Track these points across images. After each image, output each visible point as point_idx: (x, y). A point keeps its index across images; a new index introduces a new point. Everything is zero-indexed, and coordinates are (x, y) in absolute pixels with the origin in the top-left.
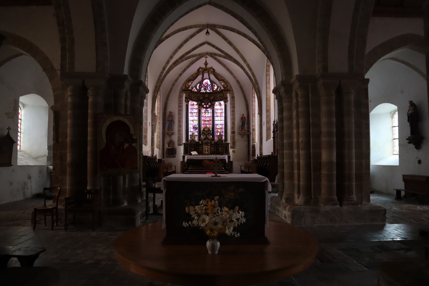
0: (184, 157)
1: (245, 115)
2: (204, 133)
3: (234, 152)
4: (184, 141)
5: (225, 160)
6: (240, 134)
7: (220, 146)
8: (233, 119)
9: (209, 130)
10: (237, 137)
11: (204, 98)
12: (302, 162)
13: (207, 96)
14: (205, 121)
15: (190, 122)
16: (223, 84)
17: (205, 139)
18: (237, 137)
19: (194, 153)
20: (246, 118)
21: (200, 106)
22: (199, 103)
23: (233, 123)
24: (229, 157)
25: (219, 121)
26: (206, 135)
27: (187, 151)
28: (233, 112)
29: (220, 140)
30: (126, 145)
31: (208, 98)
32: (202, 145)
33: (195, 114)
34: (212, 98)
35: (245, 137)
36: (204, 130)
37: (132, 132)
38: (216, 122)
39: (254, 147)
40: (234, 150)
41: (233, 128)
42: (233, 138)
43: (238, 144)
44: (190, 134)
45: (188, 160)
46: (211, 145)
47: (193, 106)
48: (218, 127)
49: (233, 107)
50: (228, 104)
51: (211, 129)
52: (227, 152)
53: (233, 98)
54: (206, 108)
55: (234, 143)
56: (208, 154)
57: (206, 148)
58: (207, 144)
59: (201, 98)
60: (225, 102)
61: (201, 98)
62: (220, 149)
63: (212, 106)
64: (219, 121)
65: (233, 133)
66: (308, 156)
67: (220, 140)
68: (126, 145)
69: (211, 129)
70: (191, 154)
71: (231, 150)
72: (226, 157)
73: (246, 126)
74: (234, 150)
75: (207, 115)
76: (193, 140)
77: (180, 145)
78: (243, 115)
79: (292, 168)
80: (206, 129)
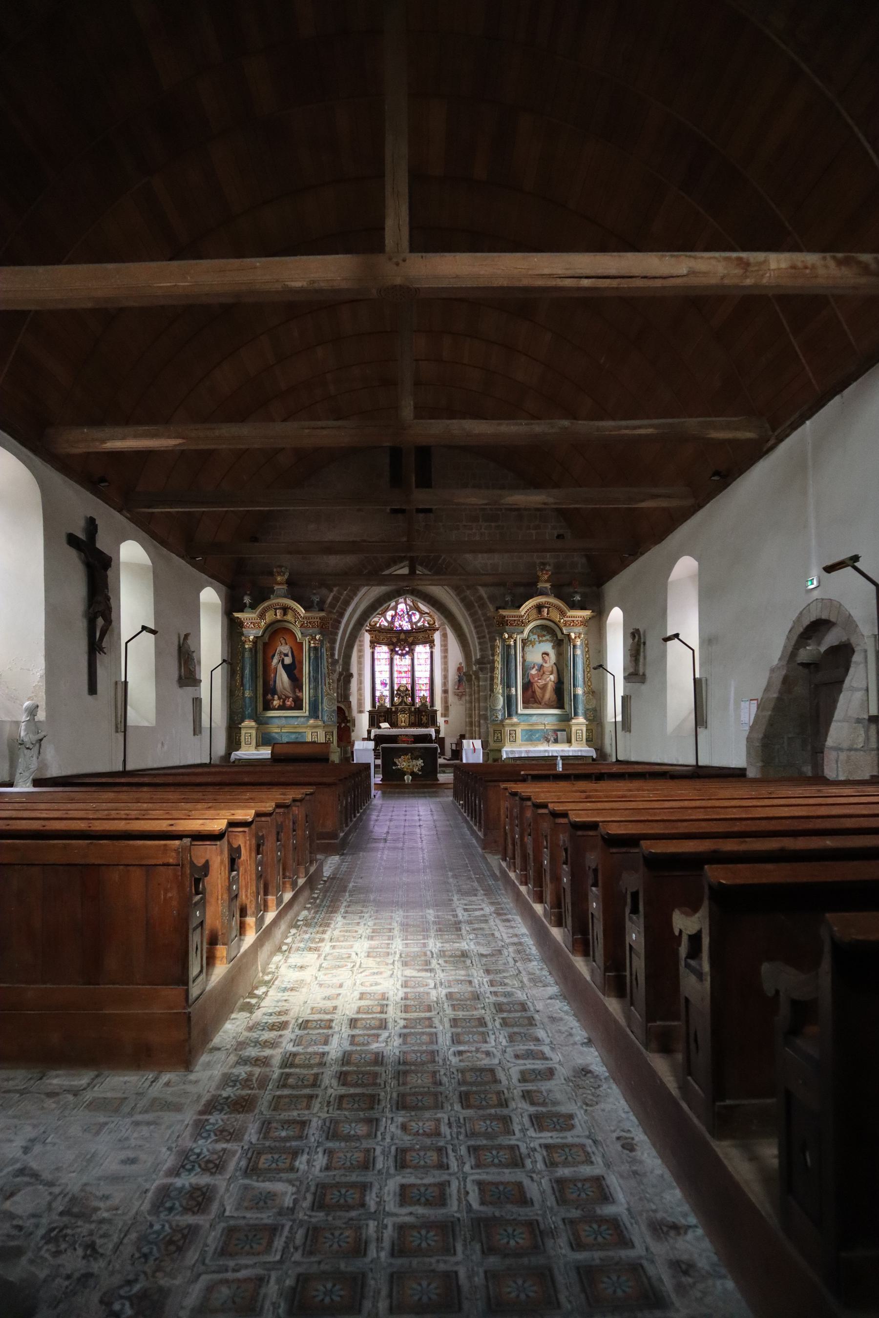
0: (369, 732)
2: (400, 695)
3: (446, 722)
4: (368, 707)
5: (431, 735)
6: (456, 694)
7: (424, 715)
8: (445, 670)
9: (407, 689)
10: (451, 698)
11: (399, 640)
13: (402, 636)
14: (400, 672)
15: (377, 675)
17: (400, 704)
19: (385, 725)
21: (393, 651)
22: (392, 647)
23: (445, 677)
25: (422, 673)
26: (403, 697)
27: (374, 722)
28: (445, 658)
29: (424, 705)
30: (343, 725)
31: (405, 641)
32: (396, 712)
33: (383, 662)
34: (410, 640)
36: (399, 690)
37: (347, 714)
38: (417, 674)
40: (446, 719)
41: (445, 684)
42: (445, 701)
43: (453, 711)
44: (378, 694)
45: (375, 736)
46: (410, 712)
47: (382, 651)
48: (421, 682)
50: (437, 650)
51: (410, 688)
54: (402, 655)
55: (446, 708)
56: (405, 727)
57: (403, 718)
58: (403, 711)
59: (395, 640)
61: (395, 640)
62: (424, 719)
63: (411, 652)
64: (422, 673)
65: (445, 692)
67: (424, 705)
68: (343, 725)
69: (410, 688)
70: (380, 728)
71: (440, 720)
72: (432, 731)
74: (446, 719)
75: (402, 663)
76: (382, 705)
77: (361, 712)
78: (460, 664)
80: (402, 689)
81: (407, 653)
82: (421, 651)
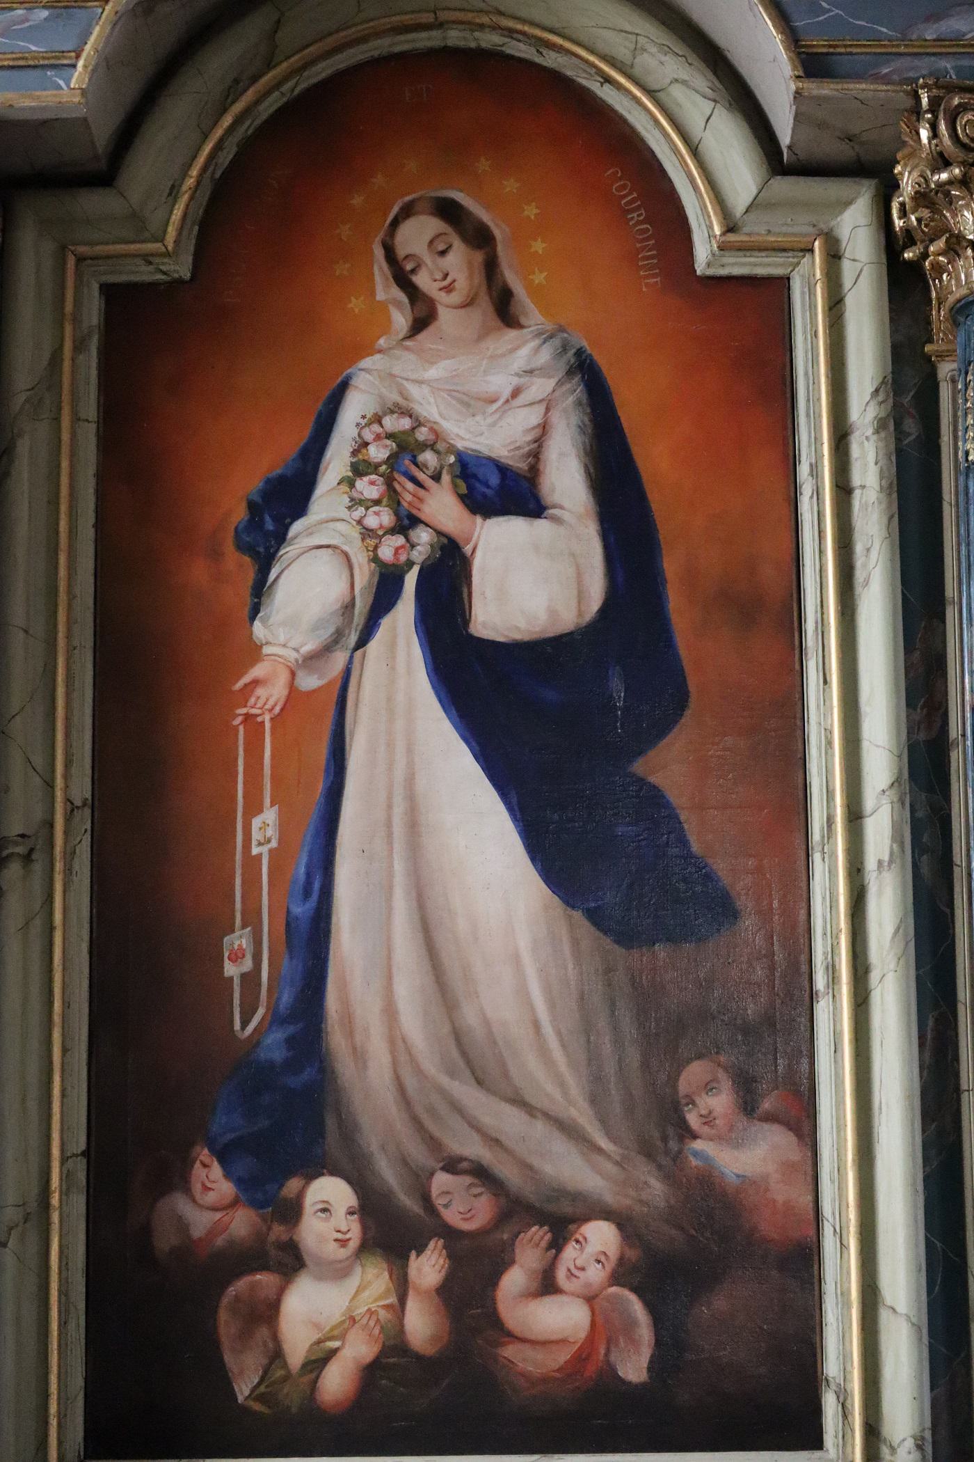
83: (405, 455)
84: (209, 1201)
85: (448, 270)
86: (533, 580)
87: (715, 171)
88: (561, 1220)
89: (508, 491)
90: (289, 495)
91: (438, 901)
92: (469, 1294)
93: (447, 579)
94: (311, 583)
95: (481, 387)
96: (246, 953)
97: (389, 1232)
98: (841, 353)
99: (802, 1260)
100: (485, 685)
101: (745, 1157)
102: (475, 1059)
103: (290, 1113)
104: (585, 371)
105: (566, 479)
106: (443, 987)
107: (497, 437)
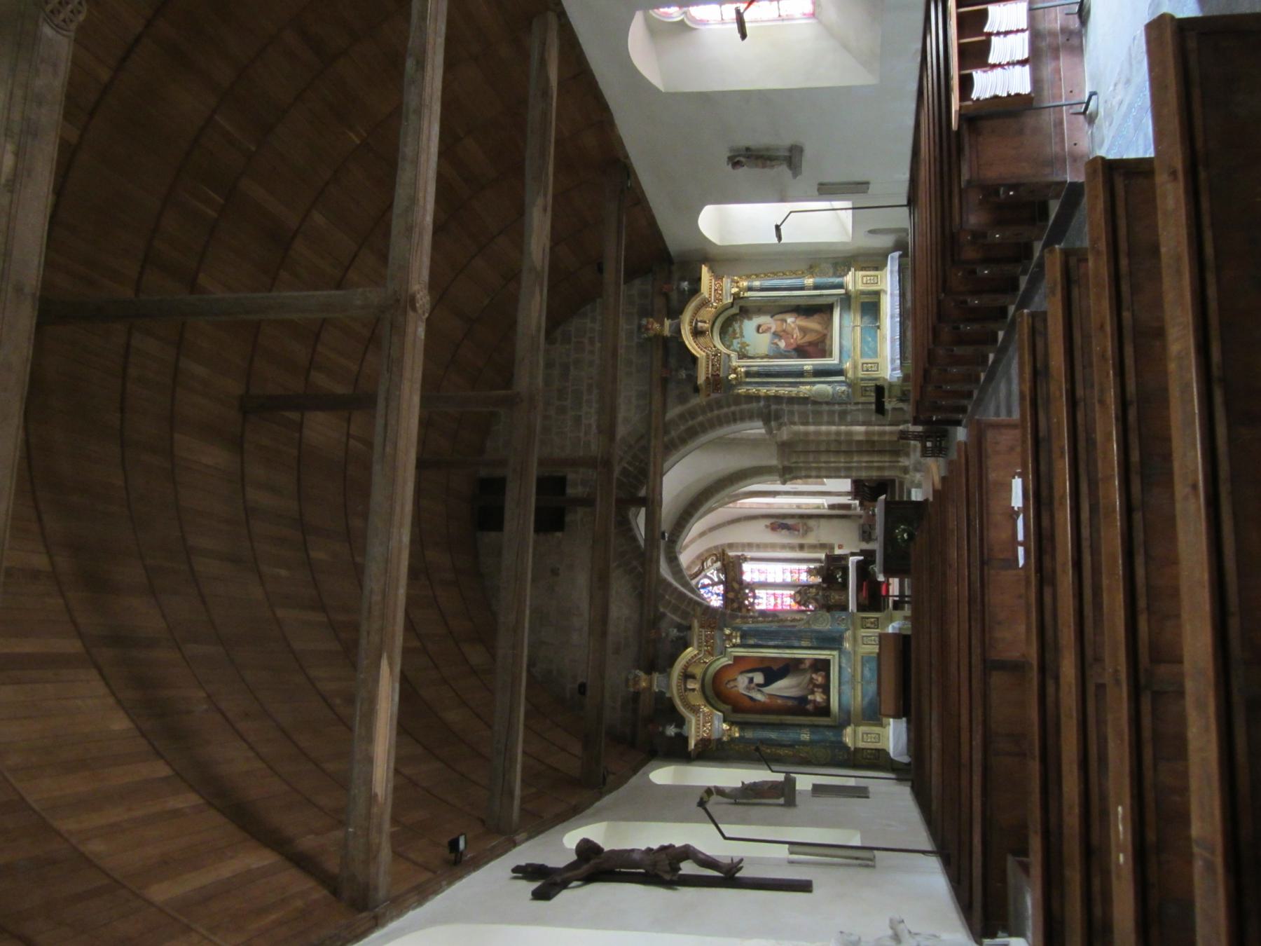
1: (768, 522)
3: (840, 547)
5: (858, 562)
8: (773, 546)
10: (811, 539)
12: (866, 458)
16: (709, 562)
18: (811, 539)
20: (773, 520)
23: (784, 547)
24: (853, 554)
29: (816, 572)
35: (812, 523)
39: (832, 507)
42: (813, 547)
49: (750, 546)
50: (749, 554)
52: (844, 558)
53: (731, 546)
54: (755, 597)
59: (735, 605)
60: (745, 559)
63: (753, 586)
65: (802, 547)
66: (860, 452)
67: (816, 572)
73: (790, 522)
79: (871, 468)
80: (798, 599)
81: (752, 590)
82: (750, 572)
83: (748, 688)
84: (810, 707)
85: (732, 684)
86: (759, 678)
87: (724, 661)
88: (812, 679)
89: (751, 680)
90: (751, 698)
91: (785, 687)
92: (818, 686)
93: (759, 685)
94: (759, 697)
95: (742, 682)
96: (790, 703)
97: (813, 692)
98: (741, 652)
99: (816, 660)
100: (769, 681)
101: (807, 664)
102: (798, 685)
103: (803, 700)
104: (742, 673)
105: (750, 675)
106: (793, 687)
107: (746, 681)
